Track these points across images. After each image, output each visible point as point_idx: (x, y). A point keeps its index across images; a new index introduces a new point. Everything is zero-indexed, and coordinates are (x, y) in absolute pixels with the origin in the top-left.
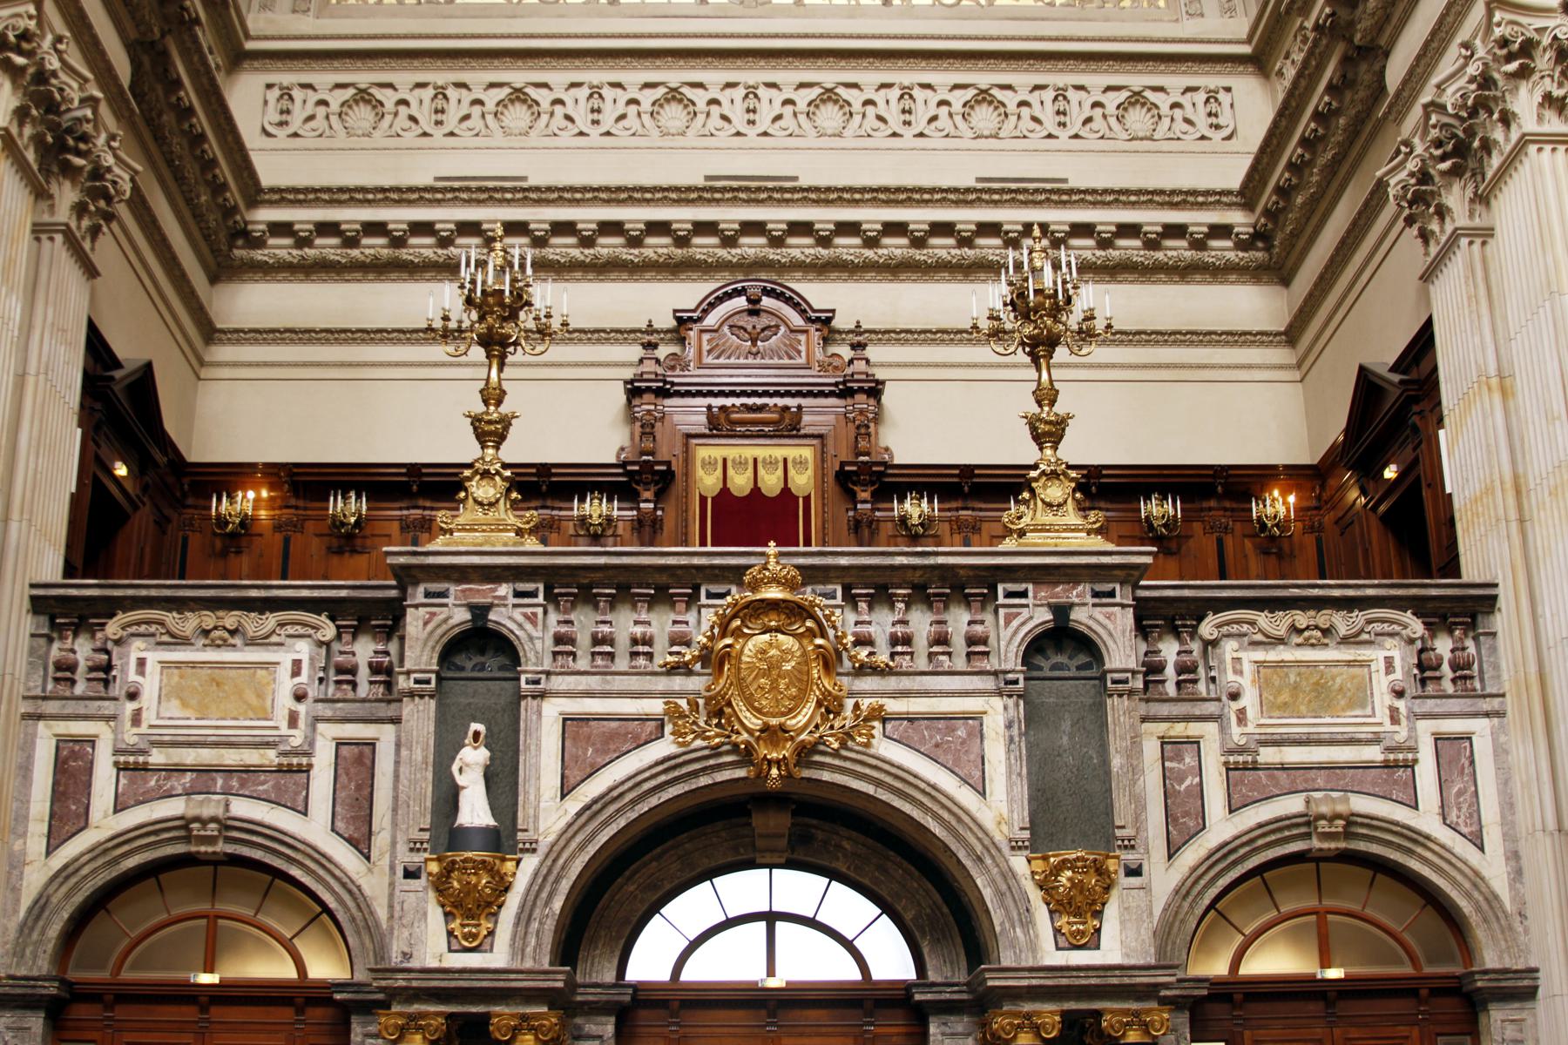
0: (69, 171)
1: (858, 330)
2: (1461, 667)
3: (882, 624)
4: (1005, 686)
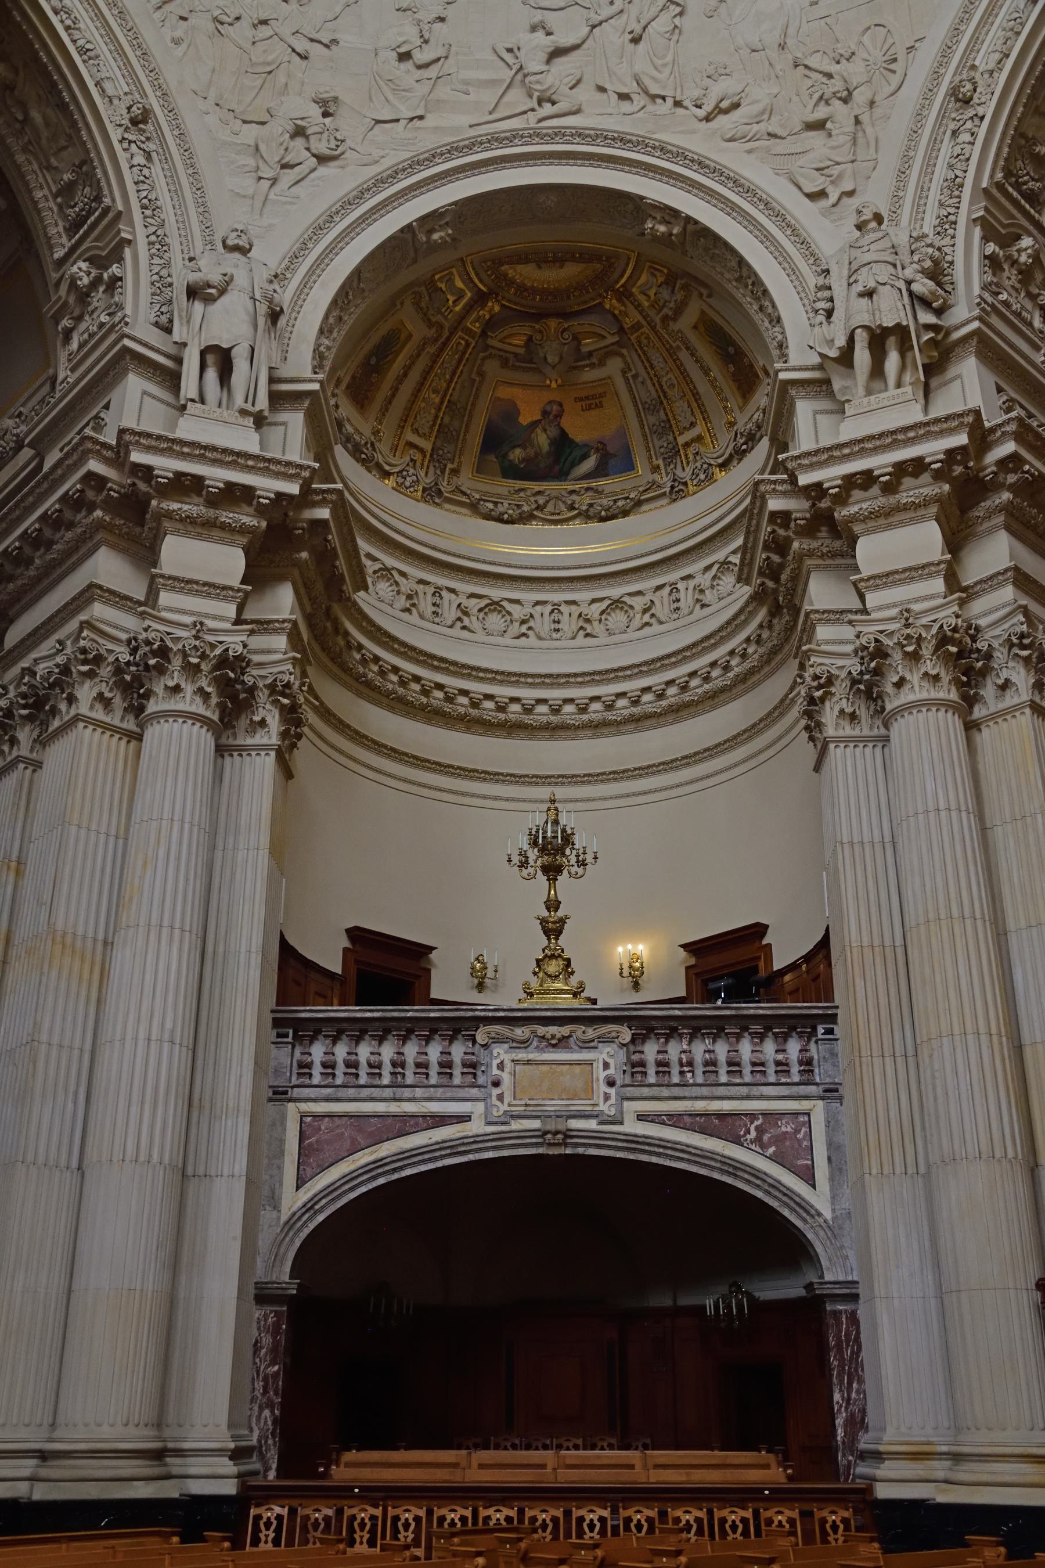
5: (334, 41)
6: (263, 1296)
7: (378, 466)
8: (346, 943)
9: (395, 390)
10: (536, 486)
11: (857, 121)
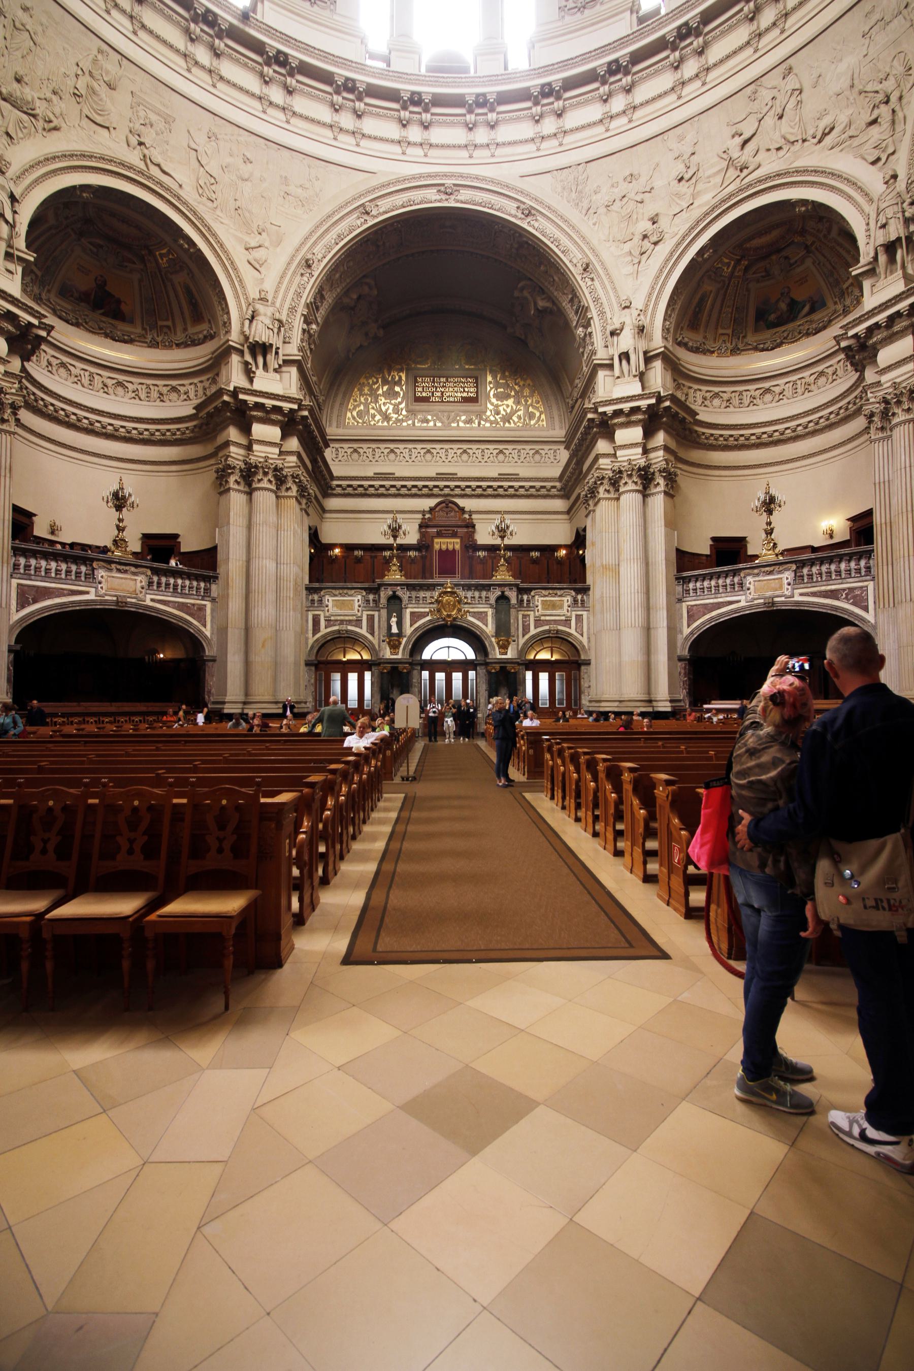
0: (304, 496)
1: (470, 511)
2: (583, 601)
3: (469, 594)
4: (491, 607)
5: (652, 188)
6: (680, 659)
7: (709, 351)
8: (711, 543)
9: (710, 316)
10: (783, 328)
11: (894, 111)
